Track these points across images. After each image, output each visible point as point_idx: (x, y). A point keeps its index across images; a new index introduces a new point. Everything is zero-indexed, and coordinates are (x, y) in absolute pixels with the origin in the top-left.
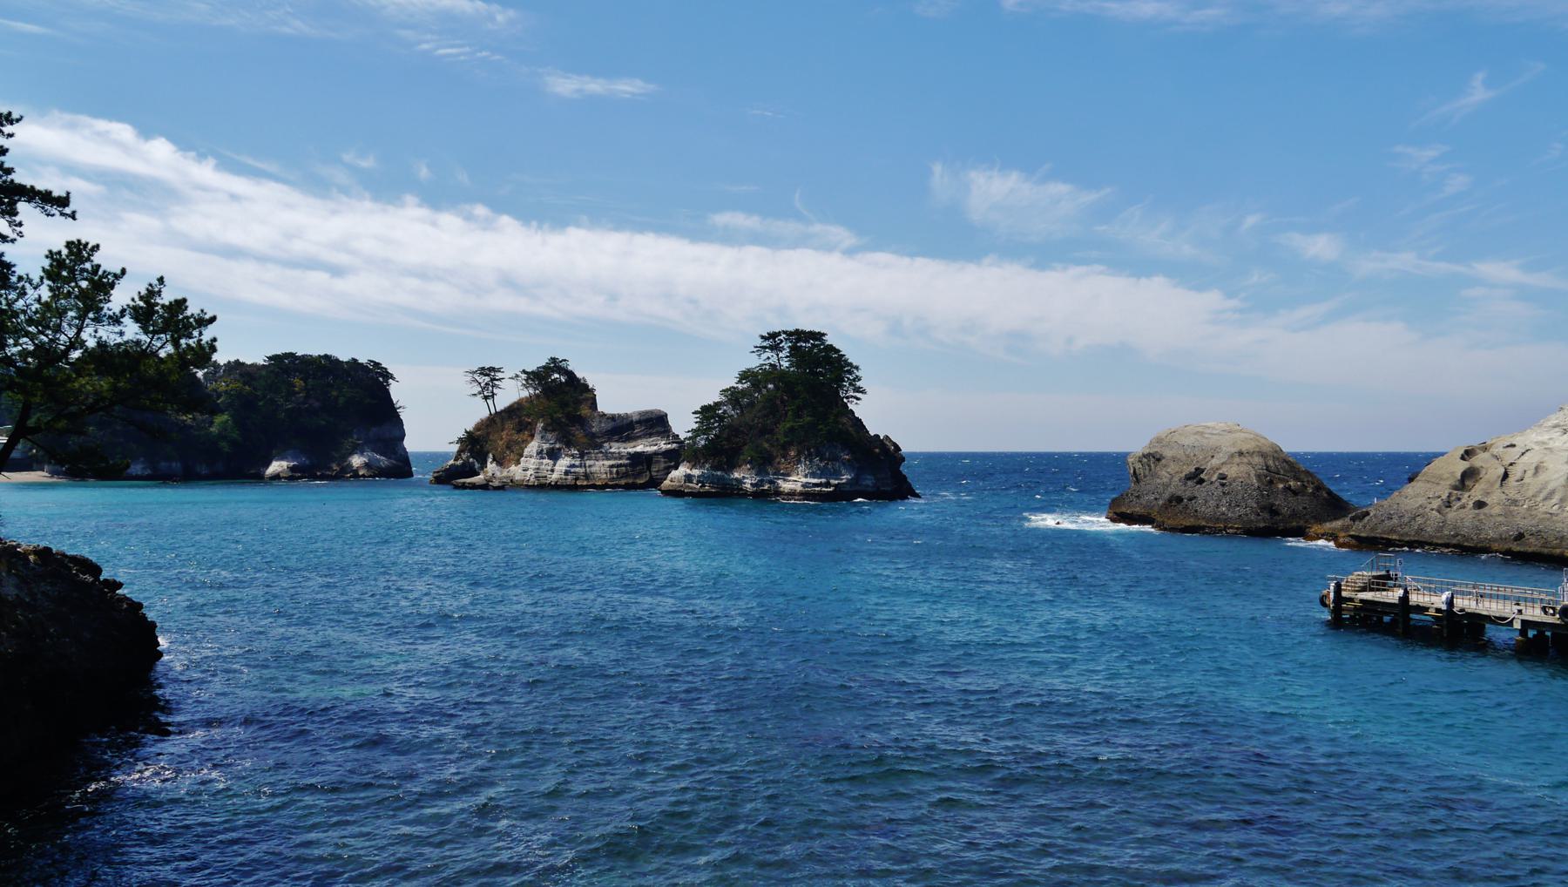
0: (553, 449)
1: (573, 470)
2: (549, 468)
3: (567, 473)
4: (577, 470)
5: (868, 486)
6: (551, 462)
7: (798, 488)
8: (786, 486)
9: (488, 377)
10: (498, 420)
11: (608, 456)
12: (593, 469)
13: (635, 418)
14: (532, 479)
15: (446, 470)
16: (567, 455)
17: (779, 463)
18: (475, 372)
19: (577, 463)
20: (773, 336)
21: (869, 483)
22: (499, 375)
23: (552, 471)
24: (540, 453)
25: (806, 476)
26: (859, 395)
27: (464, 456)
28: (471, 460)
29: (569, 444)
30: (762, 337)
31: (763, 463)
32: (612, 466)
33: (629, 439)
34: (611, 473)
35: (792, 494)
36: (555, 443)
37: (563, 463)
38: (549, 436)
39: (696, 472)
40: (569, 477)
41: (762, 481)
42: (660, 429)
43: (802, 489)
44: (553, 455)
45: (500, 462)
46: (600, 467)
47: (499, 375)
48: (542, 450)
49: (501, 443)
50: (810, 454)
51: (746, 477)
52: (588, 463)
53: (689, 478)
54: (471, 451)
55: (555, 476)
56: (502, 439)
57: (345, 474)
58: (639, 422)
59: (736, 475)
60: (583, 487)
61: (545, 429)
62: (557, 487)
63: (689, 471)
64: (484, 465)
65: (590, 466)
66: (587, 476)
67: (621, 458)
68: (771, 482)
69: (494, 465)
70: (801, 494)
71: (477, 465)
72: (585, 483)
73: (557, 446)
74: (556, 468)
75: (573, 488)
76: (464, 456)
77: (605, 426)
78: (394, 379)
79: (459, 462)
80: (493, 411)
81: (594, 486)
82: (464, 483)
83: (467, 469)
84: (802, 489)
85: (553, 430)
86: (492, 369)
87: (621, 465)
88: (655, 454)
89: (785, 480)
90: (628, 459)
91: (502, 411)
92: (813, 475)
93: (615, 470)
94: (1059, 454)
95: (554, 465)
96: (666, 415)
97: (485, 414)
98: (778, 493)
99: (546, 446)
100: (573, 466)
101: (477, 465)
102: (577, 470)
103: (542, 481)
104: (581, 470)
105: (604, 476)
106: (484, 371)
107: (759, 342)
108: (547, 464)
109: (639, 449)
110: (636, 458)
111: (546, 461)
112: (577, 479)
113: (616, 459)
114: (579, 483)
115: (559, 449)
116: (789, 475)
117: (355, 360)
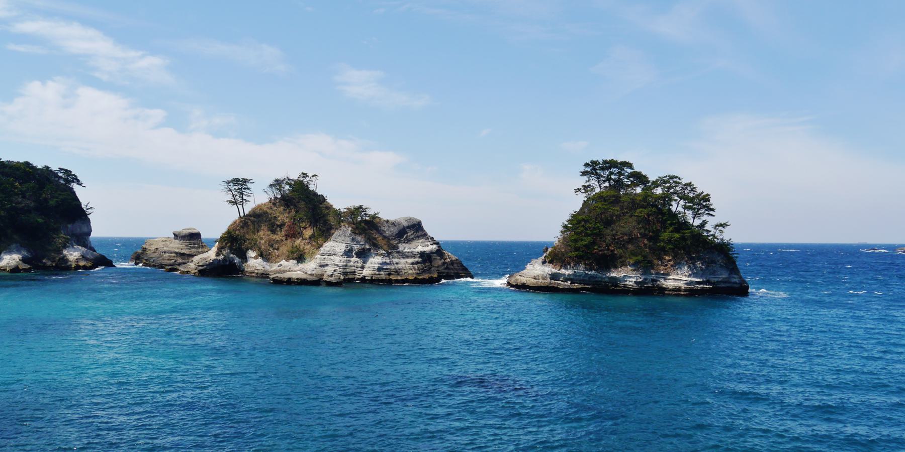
0: (364, 249)
1: (385, 267)
2: (359, 265)
3: (379, 269)
4: (388, 267)
5: (735, 283)
6: (360, 261)
7: (683, 285)
8: (670, 283)
9: (240, 185)
10: (249, 223)
11: (404, 255)
12: (400, 266)
13: (405, 224)
14: (336, 274)
15: (210, 264)
16: (377, 255)
17: (658, 265)
18: (228, 182)
19: (388, 261)
20: (594, 163)
21: (737, 280)
22: (249, 185)
23: (363, 267)
24: (348, 253)
25: (689, 276)
26: (711, 212)
27: (225, 253)
28: (232, 255)
29: (376, 246)
30: (587, 165)
31: (644, 265)
32: (413, 264)
33: (408, 241)
34: (414, 268)
35: (677, 290)
36: (365, 244)
37: (375, 261)
38: (359, 238)
39: (566, 272)
40: (382, 273)
41: (645, 279)
42: (420, 233)
43: (685, 286)
44: (363, 254)
45: (264, 255)
46: (406, 265)
47: (249, 185)
48: (351, 251)
49: (263, 241)
50: (692, 259)
51: (628, 276)
52: (395, 260)
53: (554, 276)
54: (230, 248)
55: (367, 272)
56: (262, 239)
57: (63, 267)
58: (408, 227)
59: (614, 274)
60: (397, 281)
61: (354, 232)
62: (371, 282)
63: (555, 271)
64: (244, 258)
65: (397, 263)
66: (397, 272)
67: (414, 256)
68: (654, 281)
69: (260, 260)
70: (685, 290)
71: (237, 260)
72: (399, 278)
73: (367, 247)
74: (368, 265)
75: (388, 283)
76: (225, 253)
77: (395, 230)
78: (79, 183)
79: (221, 257)
80: (242, 215)
81: (407, 280)
82: (289, 279)
83: (228, 263)
84: (685, 286)
85: (360, 234)
86: (245, 181)
87: (417, 263)
88: (432, 253)
89: (665, 279)
90: (420, 257)
91: (249, 215)
92: (695, 275)
93: (416, 266)
94: (499, 242)
95: (365, 262)
96: (421, 222)
97: (236, 217)
98: (662, 290)
99: (356, 247)
100: (385, 263)
101: (237, 260)
102: (388, 267)
103: (350, 276)
104: (392, 267)
105: (410, 272)
106: (236, 181)
107: (583, 169)
108: (357, 262)
109: (420, 249)
110: (422, 254)
111: (354, 259)
112: (389, 274)
113: (412, 257)
114: (391, 277)
115: (369, 250)
116: (668, 274)
117: (47, 168)
